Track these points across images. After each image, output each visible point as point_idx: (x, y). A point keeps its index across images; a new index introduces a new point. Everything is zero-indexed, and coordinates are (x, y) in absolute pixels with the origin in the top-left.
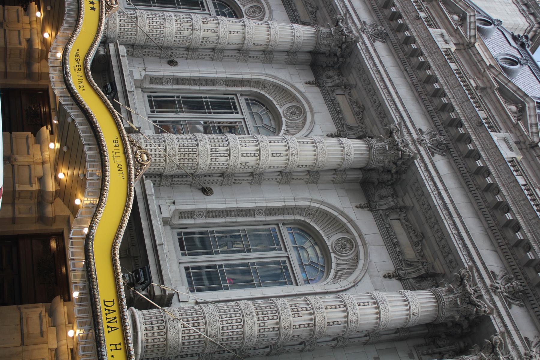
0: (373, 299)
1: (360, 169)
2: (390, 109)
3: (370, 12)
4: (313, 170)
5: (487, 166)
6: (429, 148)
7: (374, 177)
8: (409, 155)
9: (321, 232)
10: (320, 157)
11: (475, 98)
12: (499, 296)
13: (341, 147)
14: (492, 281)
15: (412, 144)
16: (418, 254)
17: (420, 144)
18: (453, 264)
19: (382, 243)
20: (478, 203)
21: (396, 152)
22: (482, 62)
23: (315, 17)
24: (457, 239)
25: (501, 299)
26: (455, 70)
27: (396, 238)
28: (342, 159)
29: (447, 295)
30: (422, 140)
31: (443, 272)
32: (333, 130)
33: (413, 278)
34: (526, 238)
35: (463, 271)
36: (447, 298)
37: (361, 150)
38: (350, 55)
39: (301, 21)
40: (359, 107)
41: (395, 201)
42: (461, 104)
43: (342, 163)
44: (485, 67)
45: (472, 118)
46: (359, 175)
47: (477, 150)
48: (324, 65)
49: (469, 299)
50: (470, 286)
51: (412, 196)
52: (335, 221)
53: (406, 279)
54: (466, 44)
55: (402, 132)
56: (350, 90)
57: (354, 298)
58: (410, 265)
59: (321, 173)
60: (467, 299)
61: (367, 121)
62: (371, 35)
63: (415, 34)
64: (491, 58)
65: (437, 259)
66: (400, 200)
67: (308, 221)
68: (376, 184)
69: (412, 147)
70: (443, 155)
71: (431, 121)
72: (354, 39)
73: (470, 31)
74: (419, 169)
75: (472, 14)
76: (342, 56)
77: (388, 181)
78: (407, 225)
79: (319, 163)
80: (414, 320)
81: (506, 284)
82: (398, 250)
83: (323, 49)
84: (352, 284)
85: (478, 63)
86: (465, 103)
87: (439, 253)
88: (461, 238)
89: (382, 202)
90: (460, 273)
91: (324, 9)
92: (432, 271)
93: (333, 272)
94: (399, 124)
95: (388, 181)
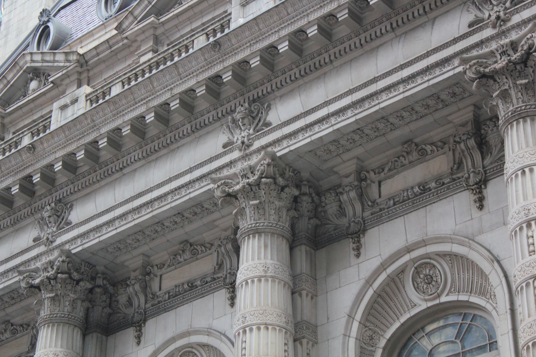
0: (521, 229)
1: (291, 249)
2: (187, 198)
3: (17, 230)
4: (293, 331)
5: (288, 35)
6: (256, 131)
7: (305, 225)
8: (269, 165)
9: (403, 320)
10: (271, 319)
11: (172, 55)
12: (512, 14)
13: (253, 282)
14: (486, 26)
15: (249, 159)
16: (441, 151)
17: (249, 146)
18: (457, 90)
19: (421, 212)
20: (351, 50)
21: (262, 186)
22: (111, 43)
23: (21, 325)
24: (413, 85)
25: (517, 11)
26: (124, 86)
27: (412, 188)
28: (273, 281)
29: (512, 102)
30: (243, 143)
31: (472, 108)
32: (222, 295)
33: (483, 159)
35: (470, 74)
36: (517, 101)
37: (259, 248)
38: (91, 265)
39: (28, 352)
40: (183, 251)
41: (347, 189)
42: (182, 78)
43: (280, 280)
44: (119, 38)
45: (206, 60)
46: (302, 252)
47: (261, 50)
48: (108, 310)
49: (518, 63)
50: (496, 62)
51: (339, 160)
52: (384, 295)
53: (485, 171)
54: (79, 69)
55: (228, 177)
56: (152, 267)
57: (521, 262)
58: (460, 165)
59: (299, 319)
60: (518, 67)
61: (208, 236)
62: (59, 228)
63: (60, 154)
64: (105, 28)
65: (450, 118)
66: (346, 181)
67: (383, 343)
68: (318, 222)
69: (254, 160)
70: (269, 107)
71: (210, 128)
72: (64, 258)
73: (57, 61)
74: (292, 148)
75: (28, 58)
76: (93, 279)
77: (313, 201)
78: (390, 170)
79: (282, 321)
81: (491, 3)
82: (433, 185)
83: (80, 313)
84: (496, 264)
85: (113, 49)
86: (181, 70)
87: (437, 115)
88: (412, 77)
89: (349, 211)
90: (473, 80)
91: (9, 310)
92: (469, 127)
93: (474, 299)
94: (214, 181)
95: (313, 201)
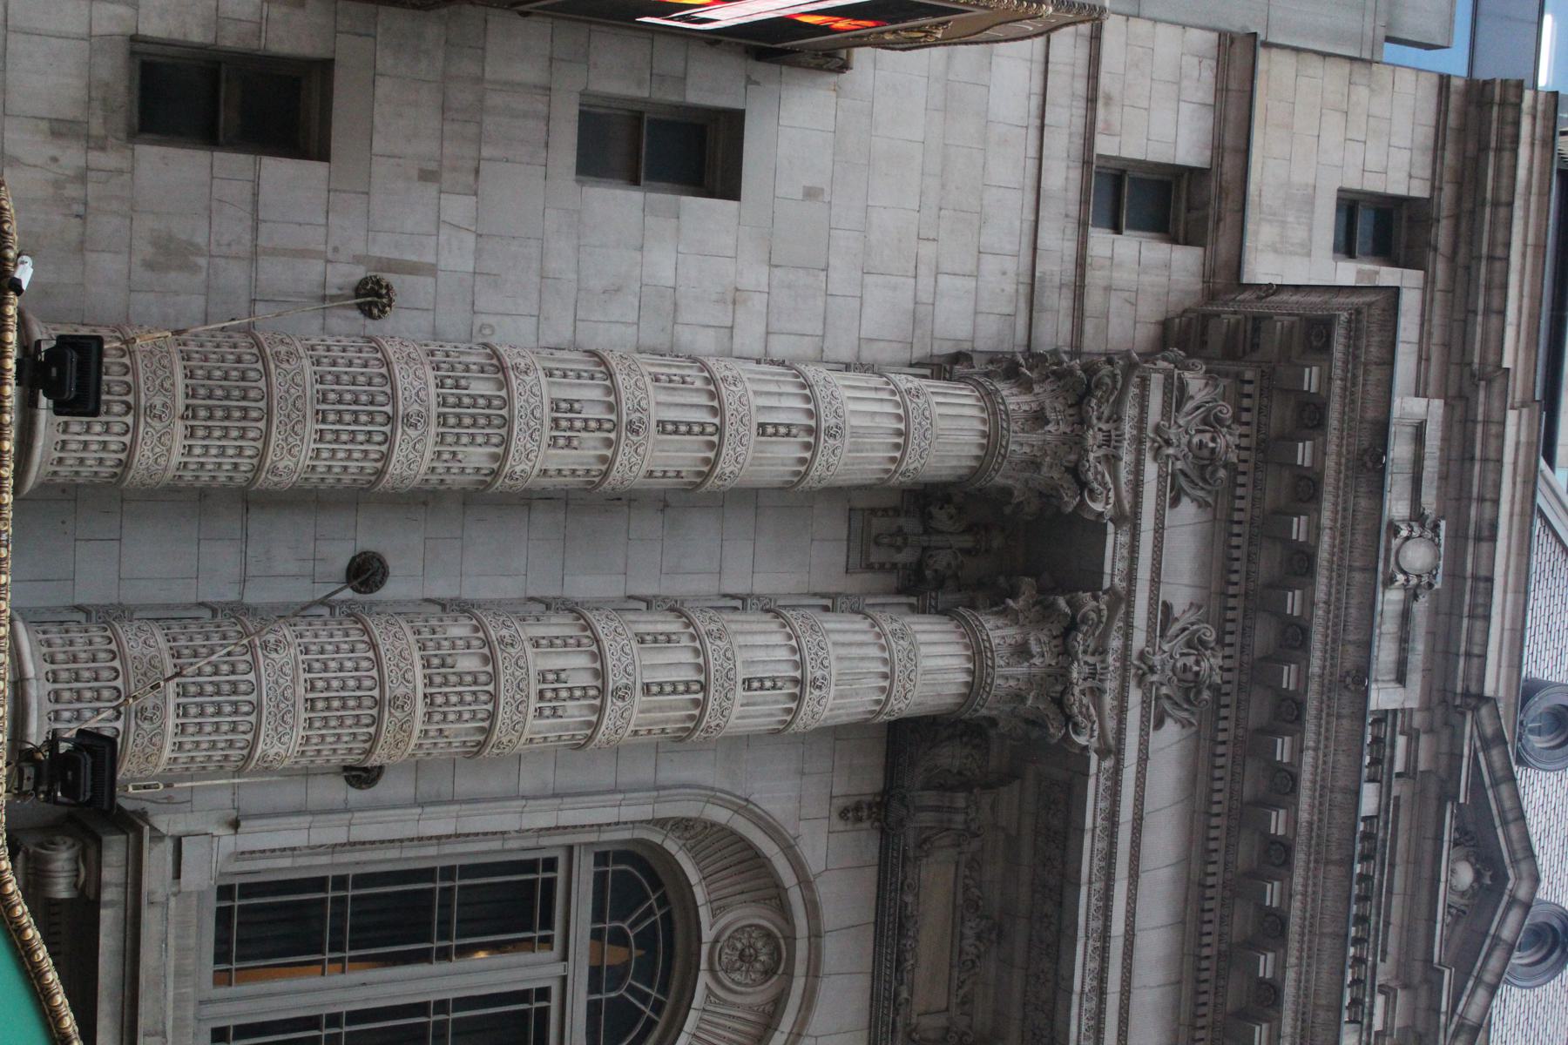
14: (1165, 413)
25: (1161, 477)
29: (1023, 430)
34: (1323, 394)
36: (1020, 443)
50: (1099, 419)
80: (897, 480)
81: (1198, 431)
